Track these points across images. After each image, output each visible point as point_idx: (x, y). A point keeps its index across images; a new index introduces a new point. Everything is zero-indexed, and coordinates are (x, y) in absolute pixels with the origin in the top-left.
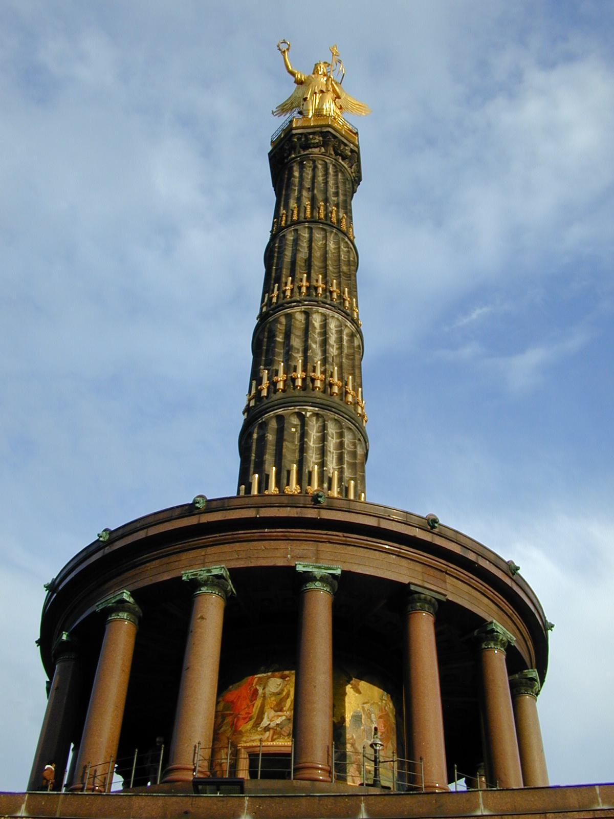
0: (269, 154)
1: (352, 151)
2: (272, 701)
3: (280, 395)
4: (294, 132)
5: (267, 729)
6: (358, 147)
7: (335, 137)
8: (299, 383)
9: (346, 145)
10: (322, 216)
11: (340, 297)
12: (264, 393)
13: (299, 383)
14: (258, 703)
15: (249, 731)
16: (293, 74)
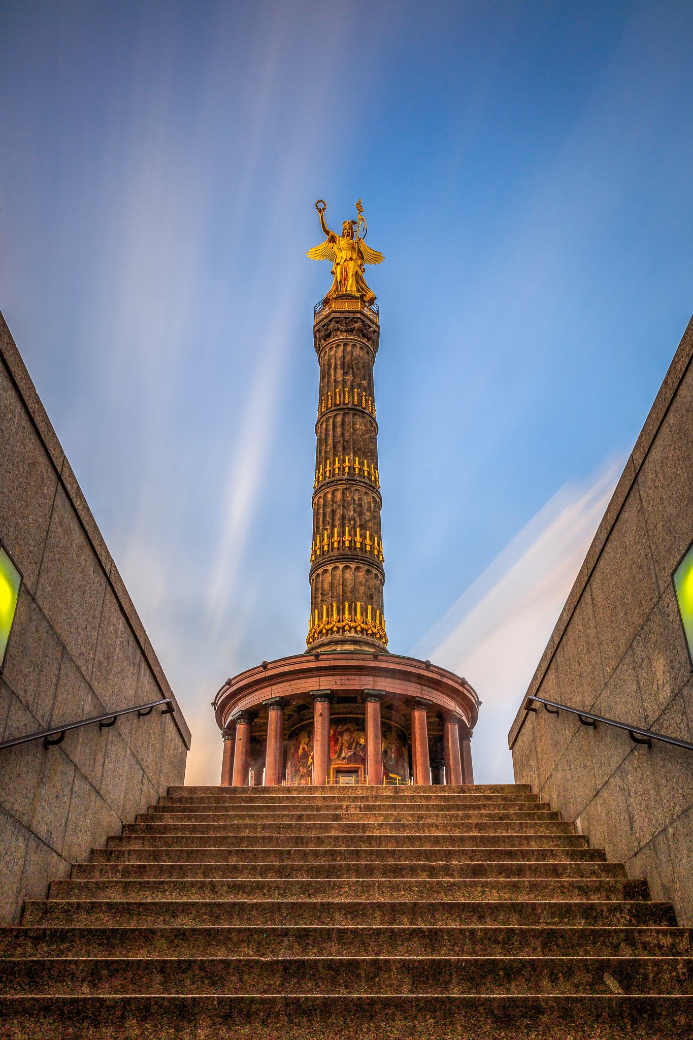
0: (314, 327)
1: (375, 331)
2: (346, 744)
3: (336, 553)
4: (333, 315)
5: (344, 758)
6: (378, 327)
7: (363, 322)
8: (347, 544)
10: (356, 403)
11: (369, 473)
12: (326, 548)
13: (347, 544)
14: (339, 745)
15: (336, 759)
16: (327, 233)
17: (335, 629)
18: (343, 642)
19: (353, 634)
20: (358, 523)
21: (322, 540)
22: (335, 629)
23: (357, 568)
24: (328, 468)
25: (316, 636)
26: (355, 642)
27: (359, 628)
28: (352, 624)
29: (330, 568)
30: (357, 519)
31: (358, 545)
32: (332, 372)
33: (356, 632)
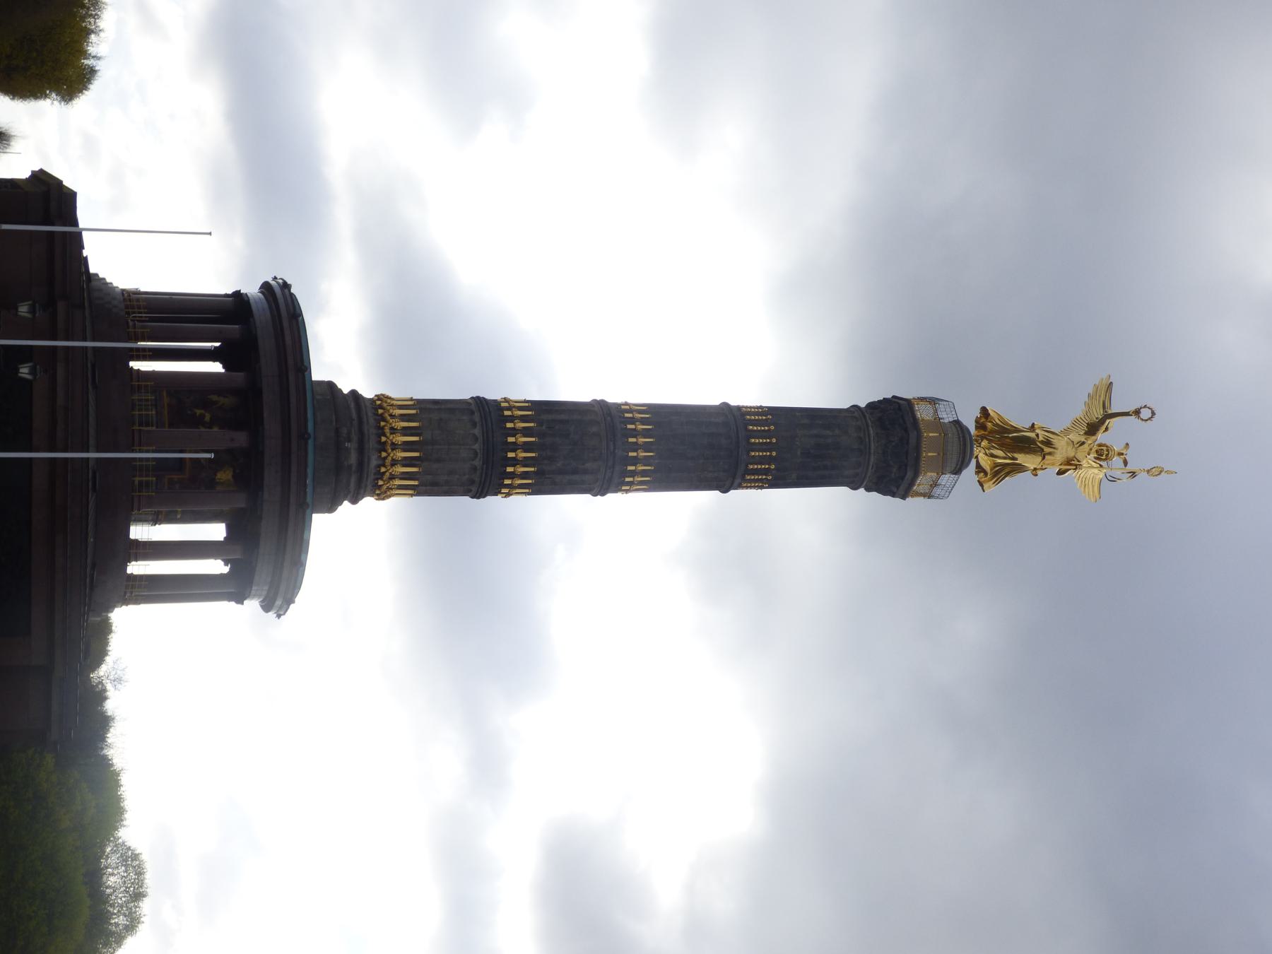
4: (913, 435)
7: (903, 478)
8: (511, 455)
12: (509, 425)
13: (511, 455)
17: (383, 439)
18: (361, 450)
19: (374, 462)
21: (524, 419)
22: (383, 439)
23: (475, 469)
24: (641, 427)
25: (380, 411)
26: (361, 464)
27: (383, 470)
28: (388, 461)
29: (477, 431)
31: (510, 469)
32: (815, 432)
33: (379, 466)
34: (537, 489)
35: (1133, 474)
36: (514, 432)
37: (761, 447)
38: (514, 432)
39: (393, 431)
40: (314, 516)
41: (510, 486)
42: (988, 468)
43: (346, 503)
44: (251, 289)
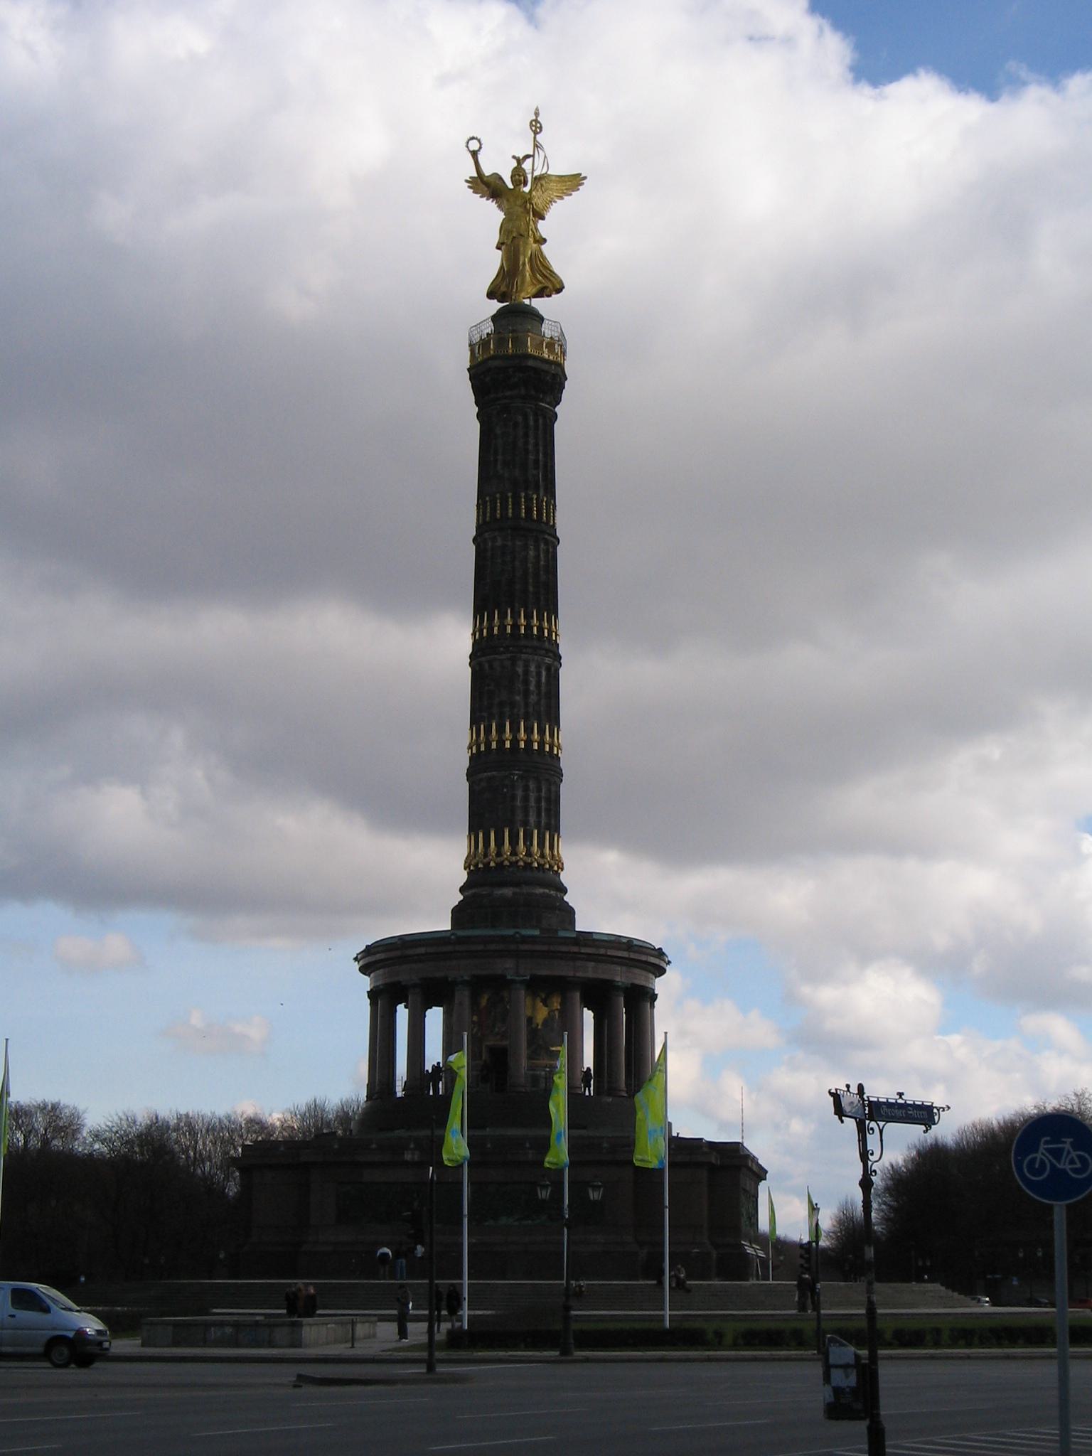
7: (535, 369)
9: (547, 372)
11: (541, 629)
12: (483, 748)
13: (508, 745)
20: (522, 711)
22: (492, 864)
28: (514, 859)
30: (522, 704)
34: (554, 719)
35: (537, 146)
36: (488, 744)
37: (504, 508)
38: (488, 744)
39: (486, 855)
40: (579, 927)
41: (542, 744)
42: (539, 286)
43: (566, 898)
44: (365, 983)
